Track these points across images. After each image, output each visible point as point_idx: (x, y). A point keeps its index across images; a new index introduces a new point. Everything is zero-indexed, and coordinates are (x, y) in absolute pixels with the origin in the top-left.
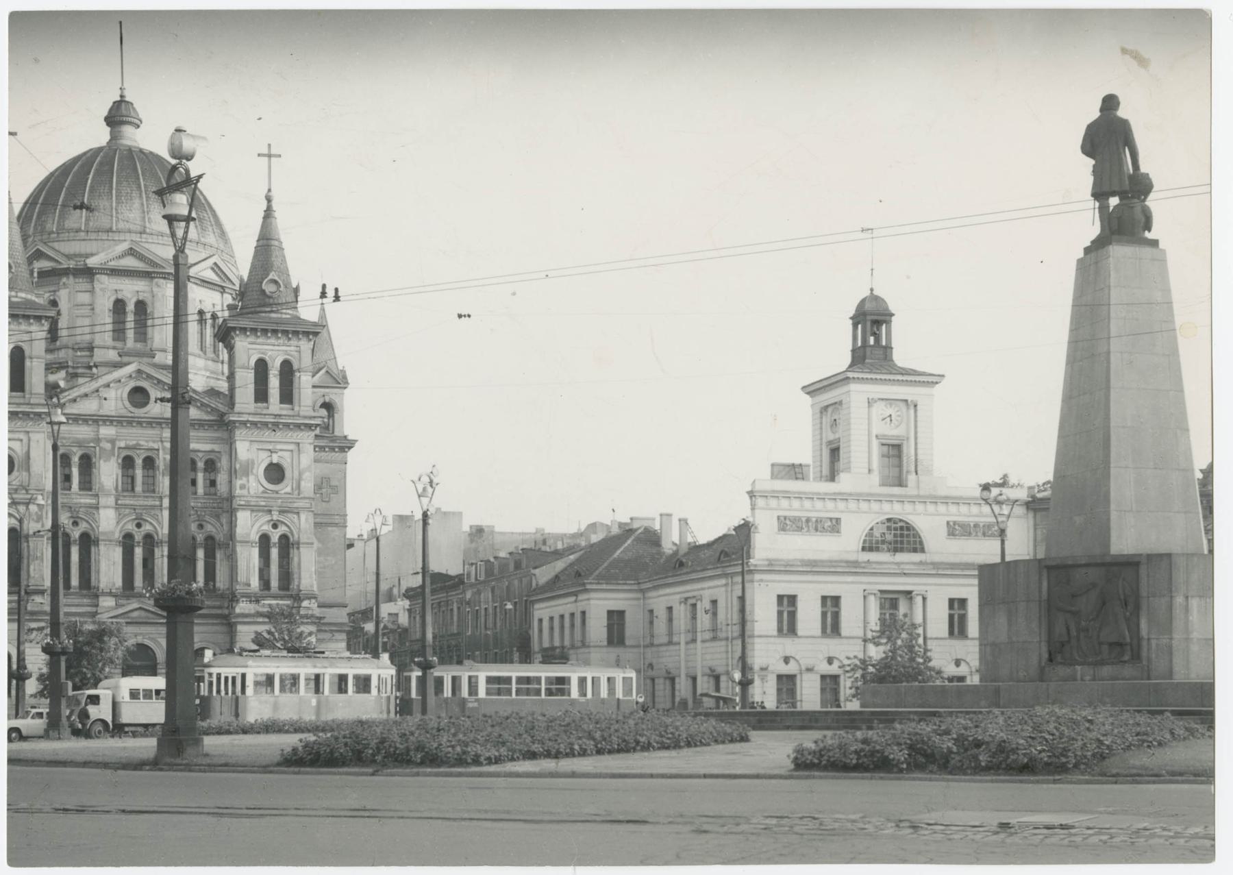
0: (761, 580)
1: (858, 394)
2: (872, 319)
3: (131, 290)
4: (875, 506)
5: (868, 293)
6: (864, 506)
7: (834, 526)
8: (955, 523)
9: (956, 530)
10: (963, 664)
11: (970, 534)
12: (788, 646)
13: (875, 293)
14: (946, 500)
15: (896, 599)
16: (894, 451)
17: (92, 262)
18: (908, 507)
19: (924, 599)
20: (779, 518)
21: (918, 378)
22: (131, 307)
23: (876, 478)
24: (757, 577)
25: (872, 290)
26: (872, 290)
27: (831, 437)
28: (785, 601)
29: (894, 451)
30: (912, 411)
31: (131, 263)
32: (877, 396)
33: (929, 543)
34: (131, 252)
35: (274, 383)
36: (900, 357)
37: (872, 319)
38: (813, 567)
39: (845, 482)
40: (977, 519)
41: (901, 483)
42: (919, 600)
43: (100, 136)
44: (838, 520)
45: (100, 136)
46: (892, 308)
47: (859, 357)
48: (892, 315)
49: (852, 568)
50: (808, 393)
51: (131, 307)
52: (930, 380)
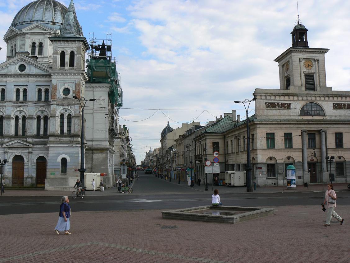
0: (259, 127)
1: (296, 57)
2: (300, 34)
3: (37, 39)
4: (305, 98)
5: (297, 24)
6: (300, 98)
7: (289, 106)
8: (336, 104)
9: (337, 107)
10: (342, 158)
11: (342, 108)
12: (272, 153)
13: (300, 23)
15: (314, 134)
16: (309, 78)
17: (24, 30)
18: (318, 98)
19: (326, 133)
20: (266, 103)
21: (318, 51)
22: (37, 44)
23: (304, 88)
24: (258, 126)
25: (298, 22)
26: (298, 22)
27: (286, 75)
28: (272, 136)
29: (309, 78)
31: (37, 30)
32: (303, 57)
35: (67, 59)
36: (311, 45)
37: (300, 34)
38: (280, 123)
39: (292, 90)
40: (344, 103)
41: (314, 89)
42: (324, 133)
44: (290, 104)
46: (307, 28)
47: (295, 44)
48: (307, 30)
50: (277, 61)
51: (37, 44)
52: (324, 51)
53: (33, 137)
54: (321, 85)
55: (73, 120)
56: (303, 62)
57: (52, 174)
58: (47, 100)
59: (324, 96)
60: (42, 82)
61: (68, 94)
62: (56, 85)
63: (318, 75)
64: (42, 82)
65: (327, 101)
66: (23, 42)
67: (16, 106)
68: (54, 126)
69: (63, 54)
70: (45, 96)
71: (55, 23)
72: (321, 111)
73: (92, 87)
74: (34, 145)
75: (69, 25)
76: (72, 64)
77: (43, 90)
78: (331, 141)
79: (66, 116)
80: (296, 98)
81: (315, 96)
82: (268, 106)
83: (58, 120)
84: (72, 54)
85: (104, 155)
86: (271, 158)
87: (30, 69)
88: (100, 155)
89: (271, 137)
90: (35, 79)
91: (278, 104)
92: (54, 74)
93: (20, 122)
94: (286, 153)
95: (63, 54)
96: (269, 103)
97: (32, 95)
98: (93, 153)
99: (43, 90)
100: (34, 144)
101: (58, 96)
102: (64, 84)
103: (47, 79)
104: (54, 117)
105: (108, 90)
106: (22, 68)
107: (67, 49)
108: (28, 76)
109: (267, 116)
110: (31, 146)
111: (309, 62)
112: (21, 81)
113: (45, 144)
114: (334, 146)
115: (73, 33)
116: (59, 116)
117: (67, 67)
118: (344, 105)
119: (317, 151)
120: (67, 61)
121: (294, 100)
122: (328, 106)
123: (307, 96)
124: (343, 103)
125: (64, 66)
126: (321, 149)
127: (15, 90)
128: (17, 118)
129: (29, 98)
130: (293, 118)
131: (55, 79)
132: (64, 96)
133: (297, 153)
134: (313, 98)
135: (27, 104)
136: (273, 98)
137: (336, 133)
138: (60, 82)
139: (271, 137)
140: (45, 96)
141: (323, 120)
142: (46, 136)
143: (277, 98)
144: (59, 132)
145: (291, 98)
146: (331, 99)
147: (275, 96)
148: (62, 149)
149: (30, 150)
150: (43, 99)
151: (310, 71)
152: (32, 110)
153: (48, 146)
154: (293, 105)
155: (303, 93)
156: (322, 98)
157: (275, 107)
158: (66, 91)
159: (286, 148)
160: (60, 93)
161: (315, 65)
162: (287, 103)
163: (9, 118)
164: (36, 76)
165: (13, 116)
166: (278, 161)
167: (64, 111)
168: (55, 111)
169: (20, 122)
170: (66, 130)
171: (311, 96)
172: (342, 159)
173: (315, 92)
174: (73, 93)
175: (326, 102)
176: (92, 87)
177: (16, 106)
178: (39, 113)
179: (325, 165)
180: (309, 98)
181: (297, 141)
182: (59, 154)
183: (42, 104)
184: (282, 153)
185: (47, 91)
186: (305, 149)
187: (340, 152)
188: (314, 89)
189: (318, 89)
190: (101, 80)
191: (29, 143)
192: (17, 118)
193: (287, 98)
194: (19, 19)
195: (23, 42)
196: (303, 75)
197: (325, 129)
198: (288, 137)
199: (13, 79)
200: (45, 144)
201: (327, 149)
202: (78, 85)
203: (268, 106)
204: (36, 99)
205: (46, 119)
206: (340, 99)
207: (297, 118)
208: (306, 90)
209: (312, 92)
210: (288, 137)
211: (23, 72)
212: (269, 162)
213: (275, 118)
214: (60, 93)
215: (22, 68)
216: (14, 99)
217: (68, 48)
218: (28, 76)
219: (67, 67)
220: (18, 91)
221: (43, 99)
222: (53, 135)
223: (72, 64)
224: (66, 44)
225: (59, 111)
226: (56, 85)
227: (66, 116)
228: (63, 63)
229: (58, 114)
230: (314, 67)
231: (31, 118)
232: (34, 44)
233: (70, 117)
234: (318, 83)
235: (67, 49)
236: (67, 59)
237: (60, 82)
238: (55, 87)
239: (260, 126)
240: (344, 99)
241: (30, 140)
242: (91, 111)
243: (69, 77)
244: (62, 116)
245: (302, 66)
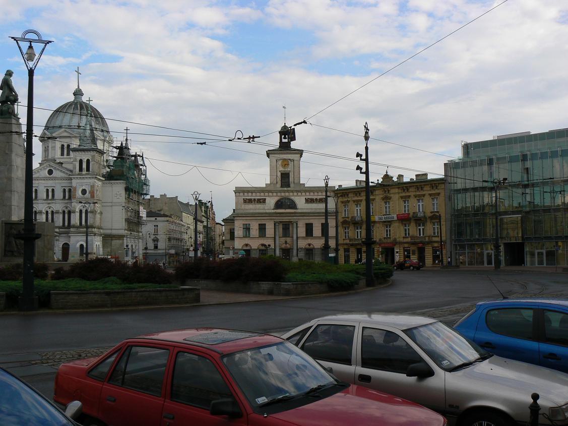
2: (288, 133)
4: (279, 194)
6: (275, 194)
7: (264, 201)
8: (308, 198)
9: (308, 201)
11: (314, 202)
12: (247, 241)
14: (306, 191)
15: (289, 224)
16: (285, 177)
17: (54, 135)
18: (291, 194)
19: (297, 224)
20: (244, 199)
22: (66, 146)
23: (279, 185)
29: (285, 177)
30: (292, 163)
33: (299, 206)
34: (65, 131)
35: (84, 166)
37: (288, 133)
38: (254, 215)
42: (295, 224)
43: (72, 98)
44: (265, 199)
45: (72, 98)
49: (270, 215)
53: (59, 228)
54: (295, 182)
55: (89, 214)
56: (280, 162)
57: (73, 257)
58: (70, 198)
59: (297, 191)
60: (65, 183)
61: (86, 193)
62: (76, 187)
63: (292, 173)
64: (65, 183)
65: (300, 196)
66: (53, 145)
67: (46, 203)
68: (75, 220)
69: (81, 161)
70: (69, 194)
71: (80, 126)
72: (293, 205)
73: (111, 183)
74: (61, 234)
75: (86, 137)
76: (88, 169)
77: (67, 190)
78: (302, 232)
79: (84, 211)
80: (270, 194)
81: (288, 191)
82: (245, 201)
83: (78, 214)
84: (88, 161)
85: (121, 241)
86: (247, 245)
87: (56, 173)
88: (118, 241)
89: (247, 229)
90: (61, 181)
91: (255, 200)
92: (74, 178)
93: (50, 216)
94: (259, 241)
95: (81, 161)
96: (246, 199)
97: (59, 194)
98: (112, 240)
99: (67, 190)
100: (60, 233)
101: (77, 196)
102: (82, 185)
103: (69, 181)
104: (74, 212)
105: (125, 186)
106: (50, 172)
107: (84, 157)
108: (55, 179)
109: (245, 209)
110: (58, 235)
111: (286, 163)
112: (50, 183)
113: (67, 233)
114: (304, 234)
115: (89, 144)
116: (79, 211)
117: (84, 172)
118: (316, 199)
119: (289, 240)
120: (85, 168)
121: (269, 196)
122: (300, 202)
123: (280, 192)
124: (315, 197)
125: (82, 171)
126: (292, 237)
127: (45, 190)
128: (47, 212)
129: (56, 197)
130: (268, 211)
131: (75, 183)
132: (82, 196)
133: (269, 241)
134: (287, 194)
135: (54, 201)
136: (250, 194)
137: (306, 224)
138: (80, 184)
139: (247, 229)
140: (69, 194)
141: (295, 213)
142: (69, 226)
143: (254, 194)
144: (78, 224)
145: (266, 194)
146: (304, 194)
147: (252, 193)
148: (80, 237)
149: (57, 237)
150: (67, 198)
151: (286, 170)
152: (58, 206)
153: (69, 235)
154: (268, 200)
155: (278, 189)
156: (295, 194)
157: (252, 202)
158: (84, 192)
159: (260, 237)
160: (79, 193)
161: (291, 164)
162: (263, 199)
163: (41, 212)
164: (62, 179)
165: (44, 211)
166: (253, 248)
167: (82, 208)
168: (75, 208)
169: (50, 216)
170: (83, 223)
171: (284, 192)
172: (311, 246)
173: (289, 189)
174: (89, 193)
175: (298, 197)
176: (111, 183)
177: (46, 203)
178: (64, 208)
179: (295, 251)
180: (283, 194)
181: (270, 230)
182: (78, 242)
183: (66, 201)
184: (257, 241)
185: (70, 191)
186: (277, 238)
187: (309, 240)
188: (289, 186)
189: (292, 185)
190: (118, 177)
191: (56, 232)
192: (47, 212)
193: (262, 194)
194: (50, 123)
195: (53, 145)
196: (279, 174)
197: (297, 220)
198: (262, 228)
199: (43, 182)
200: (67, 233)
201: (297, 237)
202: (93, 187)
203: (245, 201)
204: (62, 197)
205: (69, 213)
206: (312, 194)
207: (273, 211)
208: (147, 217)
209: (286, 189)
210: (262, 228)
211: (51, 176)
212: (245, 248)
213: (251, 211)
214: (79, 193)
215: (50, 172)
216: (45, 197)
217: (85, 157)
218: (55, 179)
219: (84, 172)
220: (47, 190)
221: (67, 198)
222: (74, 227)
223: (88, 169)
224: (83, 153)
225: (78, 207)
226: (76, 187)
227: (84, 211)
228: (81, 169)
229: (78, 210)
230: (290, 166)
231: (57, 212)
232: (63, 146)
233: (87, 212)
234: (292, 181)
235: (84, 157)
236: (84, 166)
237: (80, 184)
238: (75, 189)
239: (238, 218)
240: (316, 194)
241: (57, 230)
242: (111, 204)
243: (86, 181)
244: (81, 211)
245: (278, 166)
